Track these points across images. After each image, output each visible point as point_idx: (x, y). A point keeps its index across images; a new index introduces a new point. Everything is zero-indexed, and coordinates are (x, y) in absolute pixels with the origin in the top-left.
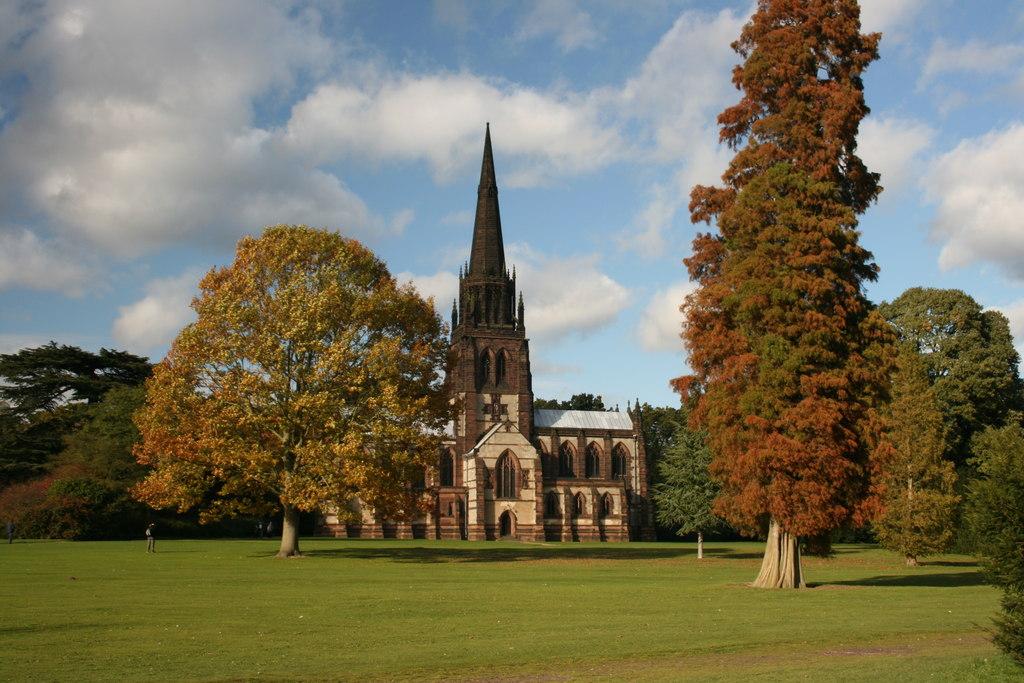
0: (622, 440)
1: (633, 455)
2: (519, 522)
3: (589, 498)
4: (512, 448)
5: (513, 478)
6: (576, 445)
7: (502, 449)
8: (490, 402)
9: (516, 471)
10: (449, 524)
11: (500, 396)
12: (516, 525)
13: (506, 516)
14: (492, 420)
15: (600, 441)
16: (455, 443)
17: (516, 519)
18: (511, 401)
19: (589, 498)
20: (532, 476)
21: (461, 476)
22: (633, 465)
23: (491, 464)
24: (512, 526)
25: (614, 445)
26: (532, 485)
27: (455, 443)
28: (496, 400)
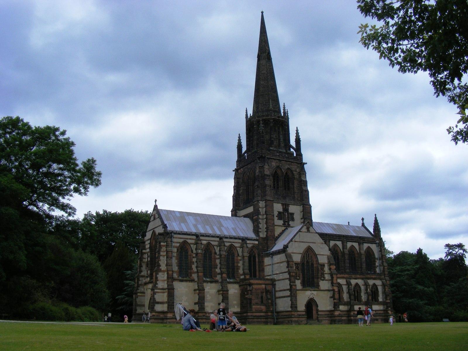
0: (370, 245)
1: (377, 256)
2: (320, 308)
3: (363, 288)
4: (312, 245)
5: (313, 271)
6: (340, 246)
7: (305, 246)
8: (281, 210)
9: (315, 265)
10: (261, 311)
11: (288, 205)
12: (317, 311)
13: (311, 304)
14: (284, 224)
15: (356, 245)
16: (257, 242)
17: (317, 306)
18: (295, 209)
19: (363, 288)
20: (326, 269)
21: (263, 270)
22: (377, 264)
23: (297, 258)
24: (314, 312)
25: (365, 248)
26: (327, 277)
27: (257, 242)
28: (286, 210)
